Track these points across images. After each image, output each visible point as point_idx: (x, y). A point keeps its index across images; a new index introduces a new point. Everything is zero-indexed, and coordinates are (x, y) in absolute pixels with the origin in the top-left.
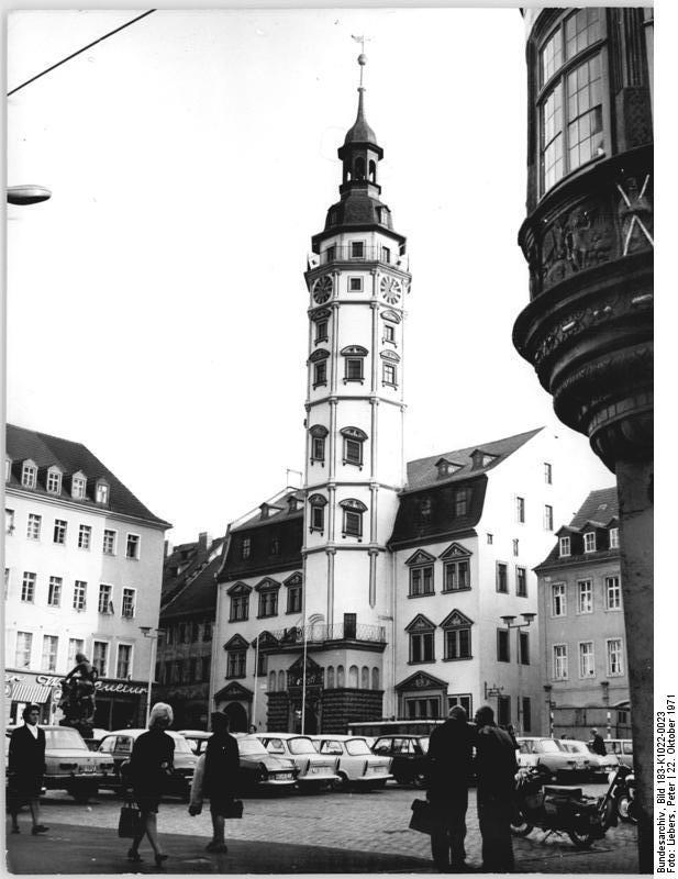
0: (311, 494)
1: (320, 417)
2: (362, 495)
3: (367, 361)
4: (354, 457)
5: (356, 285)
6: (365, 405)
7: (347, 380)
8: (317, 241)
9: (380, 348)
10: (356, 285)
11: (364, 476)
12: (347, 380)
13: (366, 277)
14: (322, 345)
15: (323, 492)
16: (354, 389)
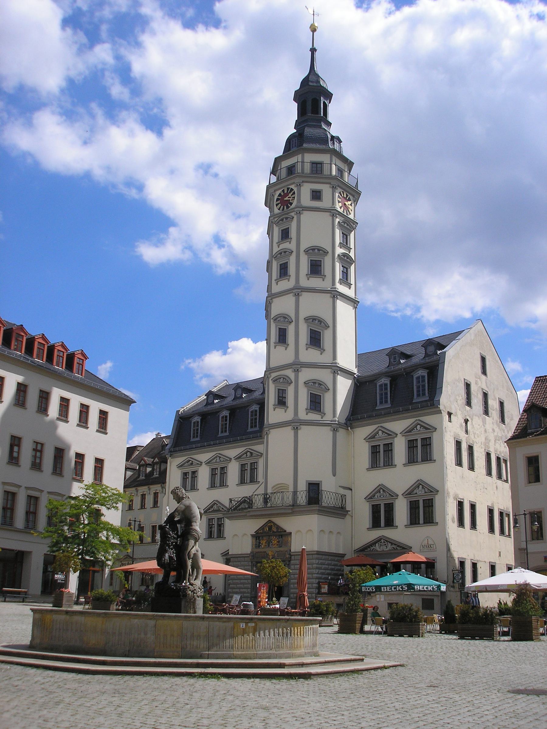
0: (274, 375)
1: (284, 305)
2: (324, 376)
3: (327, 262)
4: (315, 340)
5: (316, 195)
6: (327, 298)
7: (308, 276)
8: (278, 161)
9: (339, 251)
10: (316, 195)
11: (325, 358)
12: (308, 276)
13: (326, 190)
14: (285, 245)
15: (290, 373)
16: (315, 282)
